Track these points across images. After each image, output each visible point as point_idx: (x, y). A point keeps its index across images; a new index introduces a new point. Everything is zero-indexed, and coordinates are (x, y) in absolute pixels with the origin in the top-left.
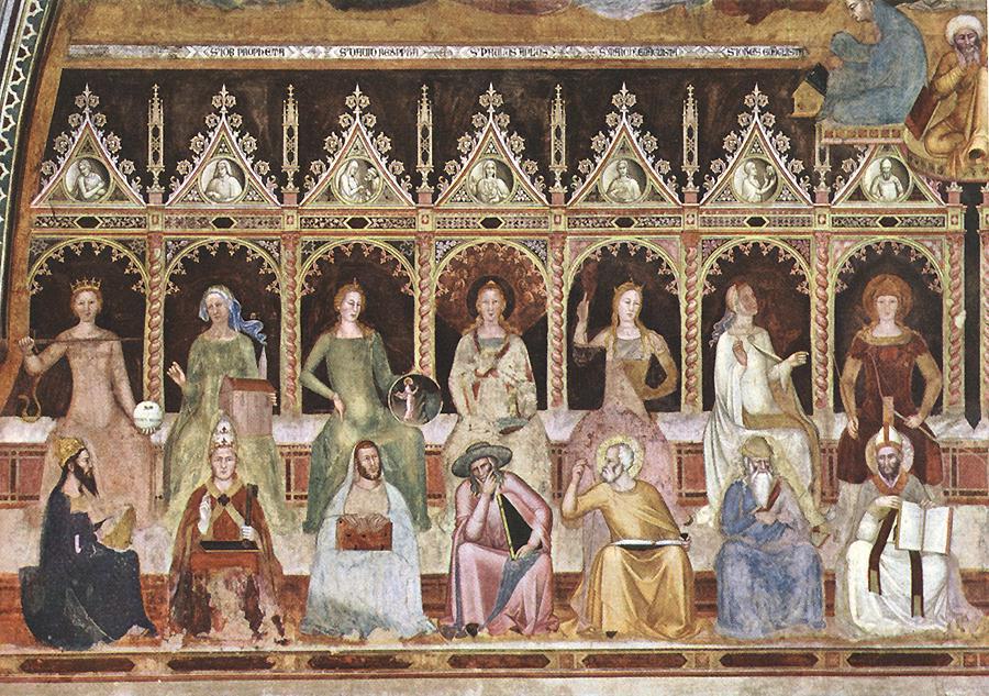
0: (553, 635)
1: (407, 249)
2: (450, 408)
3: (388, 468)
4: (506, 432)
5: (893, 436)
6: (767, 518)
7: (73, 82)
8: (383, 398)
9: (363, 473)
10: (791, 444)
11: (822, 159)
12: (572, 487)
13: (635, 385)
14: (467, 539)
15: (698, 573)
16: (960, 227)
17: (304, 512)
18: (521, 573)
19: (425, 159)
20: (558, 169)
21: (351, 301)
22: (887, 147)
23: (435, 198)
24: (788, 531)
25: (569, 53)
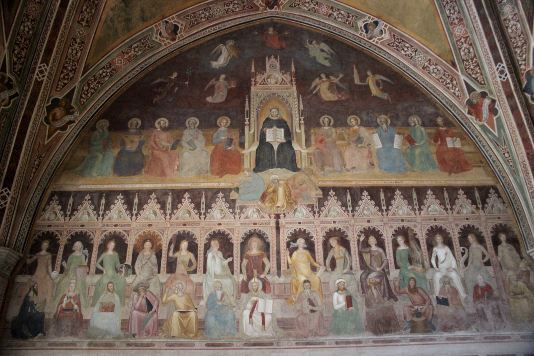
0: (157, 337)
1: (128, 232)
2: (134, 273)
3: (116, 289)
4: (148, 280)
5: (256, 280)
6: (220, 303)
7: (53, 194)
10: (227, 282)
11: (237, 208)
12: (166, 295)
13: (184, 266)
14: (135, 309)
15: (200, 319)
16: (274, 225)
17: (91, 301)
18: (148, 320)
19: (135, 210)
20: (168, 212)
21: (112, 245)
22: (254, 206)
23: (136, 219)
24: (226, 307)
25: (174, 185)
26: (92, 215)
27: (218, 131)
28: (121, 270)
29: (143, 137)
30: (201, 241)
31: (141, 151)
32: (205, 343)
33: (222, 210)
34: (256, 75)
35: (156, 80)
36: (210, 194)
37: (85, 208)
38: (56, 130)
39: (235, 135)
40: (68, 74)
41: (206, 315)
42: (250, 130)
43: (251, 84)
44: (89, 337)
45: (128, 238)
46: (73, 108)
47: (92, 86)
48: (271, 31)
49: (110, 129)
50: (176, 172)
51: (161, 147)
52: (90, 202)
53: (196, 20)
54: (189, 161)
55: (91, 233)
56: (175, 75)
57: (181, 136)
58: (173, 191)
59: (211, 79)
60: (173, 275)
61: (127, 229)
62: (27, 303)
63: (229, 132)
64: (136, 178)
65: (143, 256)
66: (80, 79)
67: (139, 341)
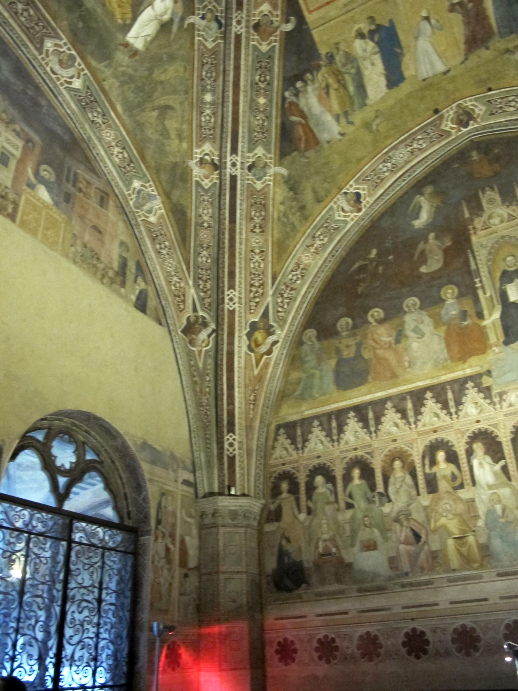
2: (390, 501)
4: (408, 505)
6: (502, 520)
7: (278, 427)
8: (370, 501)
9: (366, 526)
13: (447, 481)
15: (482, 544)
20: (412, 420)
21: (356, 472)
26: (326, 443)
27: (446, 306)
28: (374, 499)
29: (358, 338)
30: (460, 447)
31: (361, 356)
32: (495, 573)
33: (477, 403)
34: (472, 220)
35: (354, 263)
36: (456, 387)
37: (317, 436)
38: (262, 356)
39: (468, 305)
40: (257, 292)
41: (489, 538)
42: (485, 293)
43: (469, 235)
44: (356, 582)
45: (373, 461)
46: (272, 326)
47: (285, 295)
48: (475, 156)
49: (319, 338)
50: (408, 370)
51: (383, 344)
52: (320, 428)
53: (378, 178)
54: (420, 353)
55: (330, 464)
56: (374, 252)
57: (403, 323)
58: (411, 393)
59: (418, 243)
60: (435, 494)
61: (369, 450)
62: (282, 554)
63: (460, 303)
64: (364, 389)
65: (396, 478)
66: (271, 292)
67: (413, 579)
